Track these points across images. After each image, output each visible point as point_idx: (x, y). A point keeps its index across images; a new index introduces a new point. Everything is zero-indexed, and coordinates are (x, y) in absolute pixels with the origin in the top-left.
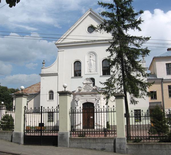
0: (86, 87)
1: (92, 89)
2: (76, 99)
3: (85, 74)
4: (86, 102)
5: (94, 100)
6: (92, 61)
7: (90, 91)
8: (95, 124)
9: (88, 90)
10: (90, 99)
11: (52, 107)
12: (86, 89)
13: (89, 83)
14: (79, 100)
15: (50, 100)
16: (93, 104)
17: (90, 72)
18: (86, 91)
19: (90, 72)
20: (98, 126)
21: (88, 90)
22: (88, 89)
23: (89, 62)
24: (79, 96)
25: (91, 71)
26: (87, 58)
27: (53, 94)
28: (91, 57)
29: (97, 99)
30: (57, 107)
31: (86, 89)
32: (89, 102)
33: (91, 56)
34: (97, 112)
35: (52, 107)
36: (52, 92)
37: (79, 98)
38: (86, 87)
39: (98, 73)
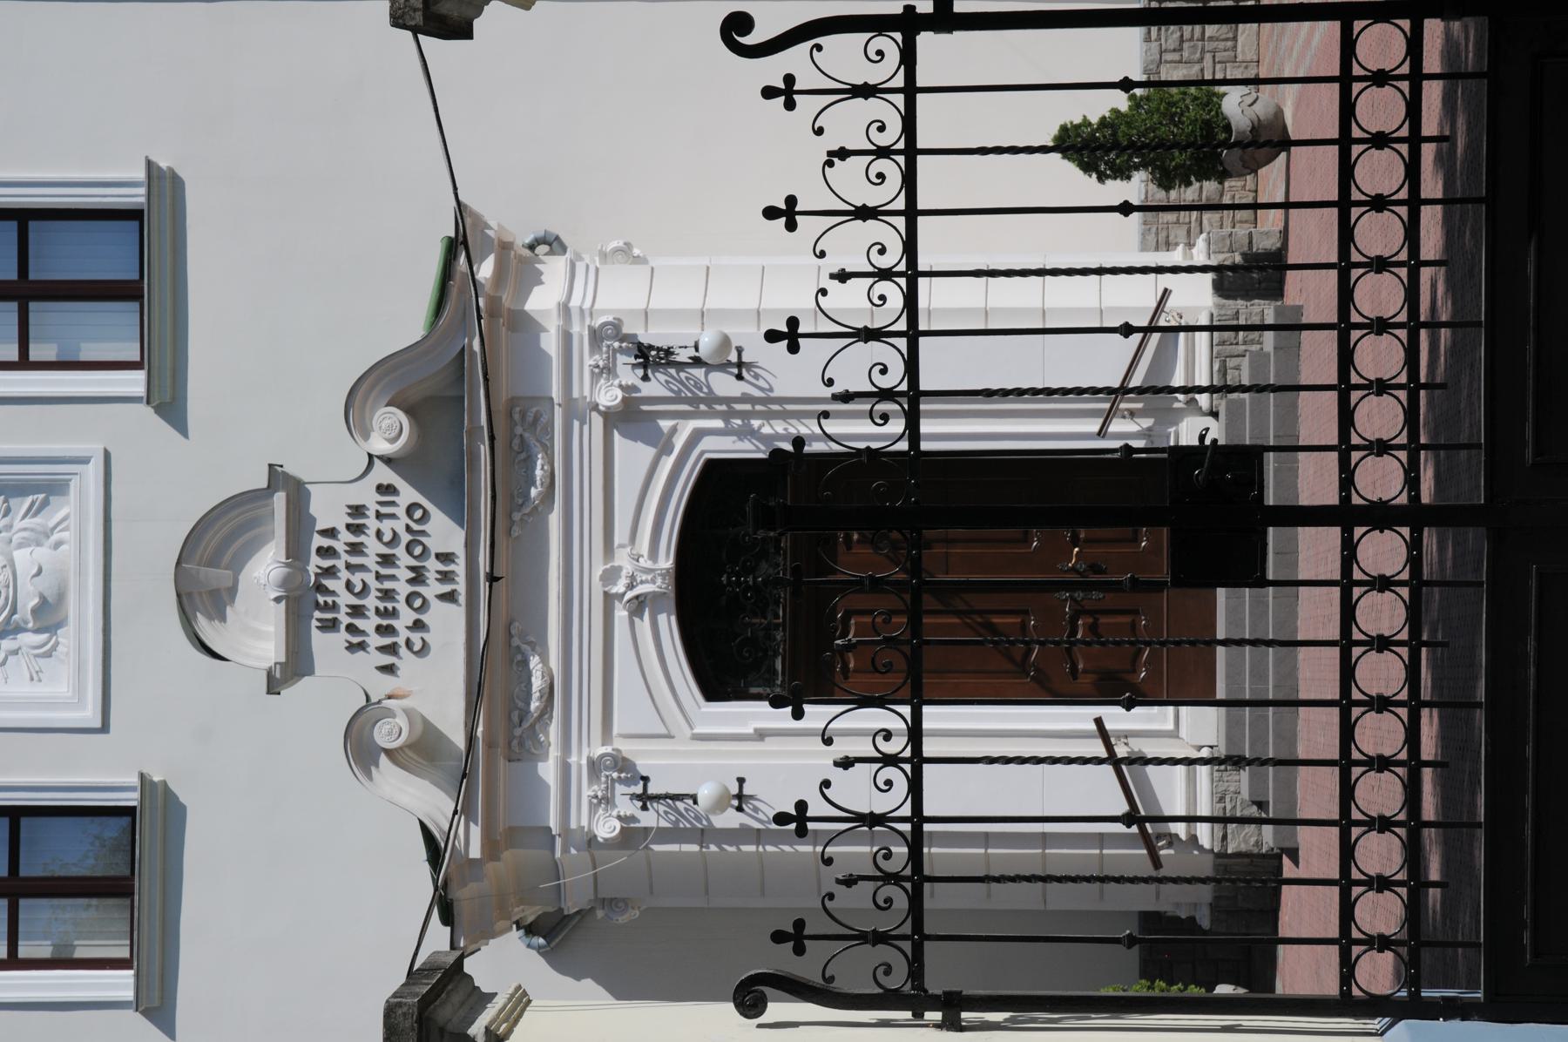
0: (368, 624)
1: (408, 494)
2: (607, 828)
3: (90, 714)
4: (668, 624)
5: (632, 455)
7: (444, 533)
8: (1128, 430)
9: (433, 565)
10: (621, 533)
11: (787, 213)
12: (407, 616)
13: (296, 551)
14: (622, 764)
16: (713, 469)
17: (49, 615)
18: (437, 606)
20: (1164, 359)
21: (433, 565)
22: (418, 577)
24: (548, 771)
25: (29, 602)
29: (609, 396)
30: (787, 93)
31: (407, 616)
32: (667, 562)
34: (913, 399)
35: (787, 213)
37: (578, 760)
39: (95, 449)
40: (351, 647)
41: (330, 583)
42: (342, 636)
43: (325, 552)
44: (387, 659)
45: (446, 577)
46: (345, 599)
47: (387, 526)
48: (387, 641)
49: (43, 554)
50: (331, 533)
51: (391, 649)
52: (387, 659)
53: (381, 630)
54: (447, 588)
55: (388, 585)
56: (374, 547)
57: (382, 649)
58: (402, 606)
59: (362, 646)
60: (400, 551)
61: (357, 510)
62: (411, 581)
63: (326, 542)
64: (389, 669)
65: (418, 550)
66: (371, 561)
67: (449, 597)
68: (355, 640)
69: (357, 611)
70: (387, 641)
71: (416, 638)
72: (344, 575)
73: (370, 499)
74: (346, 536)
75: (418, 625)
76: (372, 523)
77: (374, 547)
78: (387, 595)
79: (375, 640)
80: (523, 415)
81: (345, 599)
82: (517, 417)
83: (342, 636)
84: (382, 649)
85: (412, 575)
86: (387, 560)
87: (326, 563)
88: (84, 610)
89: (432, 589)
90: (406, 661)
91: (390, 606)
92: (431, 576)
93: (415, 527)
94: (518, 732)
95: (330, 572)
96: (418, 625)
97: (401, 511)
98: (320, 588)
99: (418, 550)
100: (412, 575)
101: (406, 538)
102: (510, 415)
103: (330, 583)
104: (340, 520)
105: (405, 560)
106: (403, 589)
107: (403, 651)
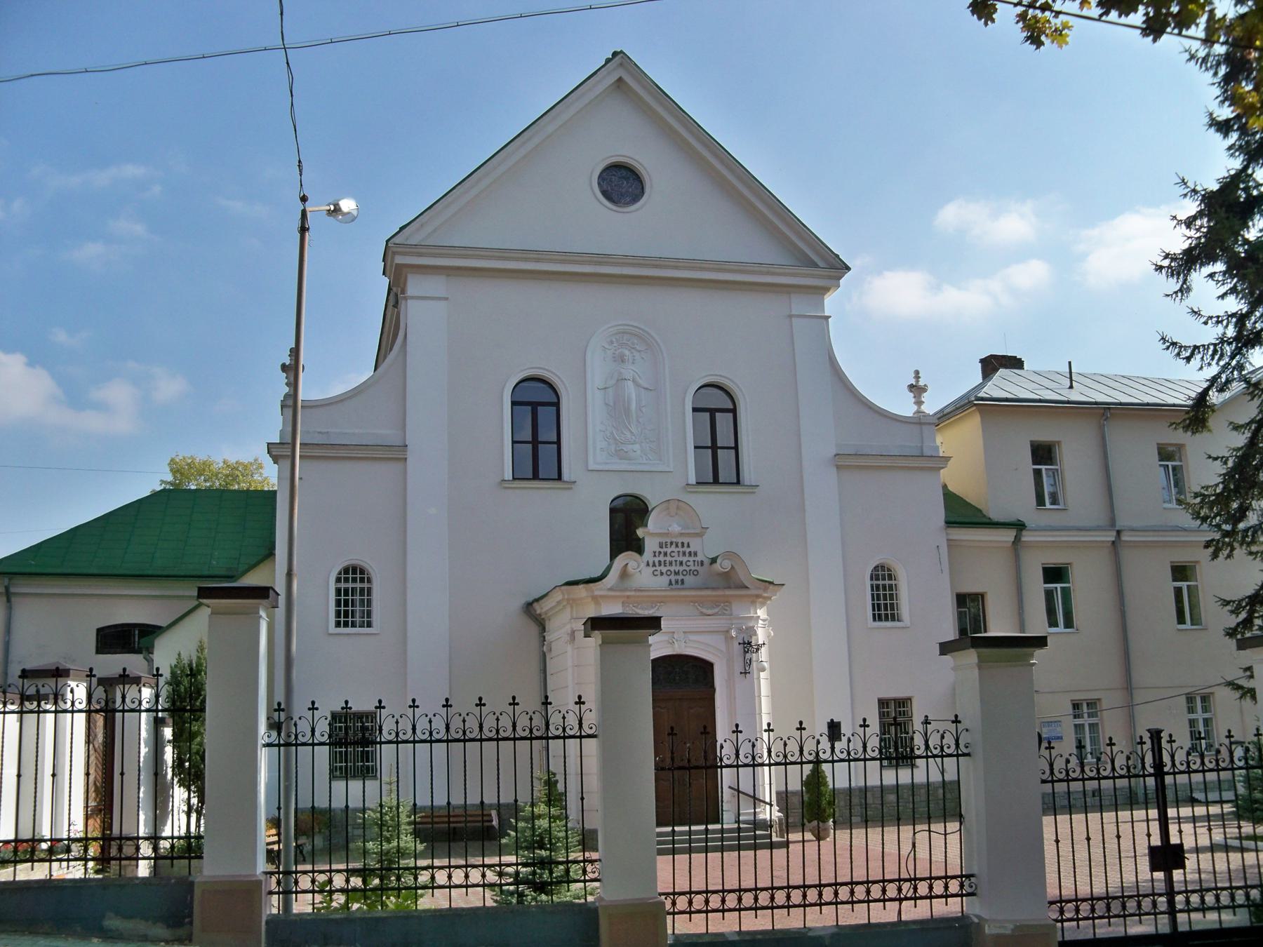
0: (662, 558)
6: (630, 388)
15: (342, 630)
17: (621, 455)
19: (621, 455)
21: (680, 577)
22: (677, 573)
23: (610, 391)
26: (598, 370)
27: (366, 585)
28: (622, 359)
31: (664, 569)
33: (627, 353)
36: (362, 572)
38: (662, 558)
40: (655, 552)
41: (674, 545)
42: (658, 549)
43: (683, 543)
44: (651, 564)
45: (677, 582)
46: (669, 550)
47: (691, 563)
48: (657, 564)
49: (639, 452)
50: (688, 546)
51: (654, 565)
52: (651, 564)
53: (660, 562)
54: (673, 582)
55: (674, 563)
56: (685, 559)
57: (654, 562)
58: (668, 568)
59: (655, 556)
60: (684, 567)
61: (696, 554)
62: (675, 571)
63: (686, 545)
64: (648, 565)
65: (685, 573)
66: (681, 558)
67: (670, 583)
68: (657, 554)
69: (665, 554)
70: (657, 564)
71: (658, 573)
72: (678, 549)
73: (699, 558)
74: (688, 550)
75: (662, 574)
76: (692, 559)
77: (685, 559)
78: (671, 564)
79: (657, 560)
80: (727, 606)
81: (669, 550)
82: (727, 604)
83: (658, 549)
84: (654, 562)
85: (677, 571)
86: (681, 563)
87: (680, 545)
88: (624, 466)
89: (673, 578)
90: (651, 569)
91: (668, 565)
92: (677, 577)
93: (691, 572)
94: (631, 606)
95: (677, 546)
96: (662, 574)
97: (696, 568)
98: (672, 543)
99: (685, 573)
100: (677, 571)
101: (688, 569)
102: (727, 602)
103: (674, 545)
104: (692, 549)
105: (681, 570)
106: (672, 569)
107: (654, 568)
